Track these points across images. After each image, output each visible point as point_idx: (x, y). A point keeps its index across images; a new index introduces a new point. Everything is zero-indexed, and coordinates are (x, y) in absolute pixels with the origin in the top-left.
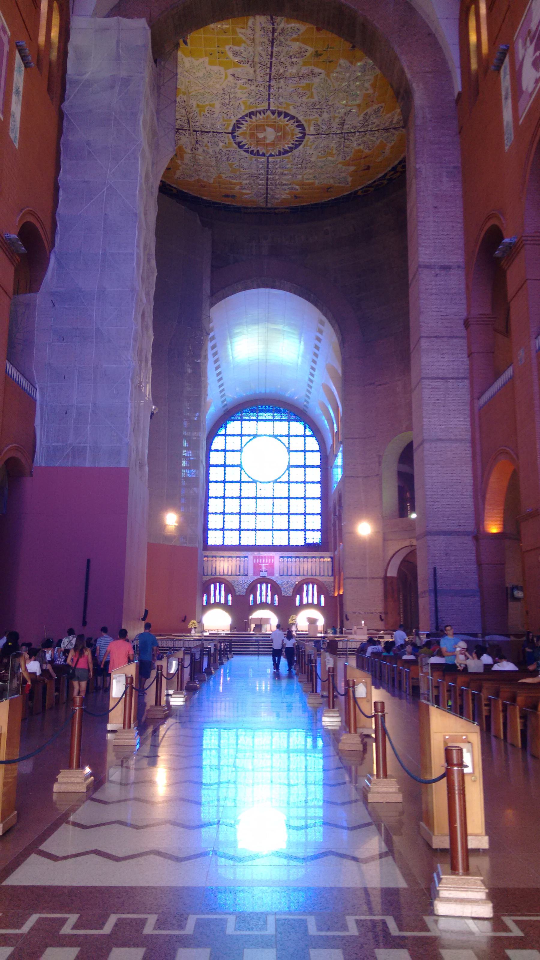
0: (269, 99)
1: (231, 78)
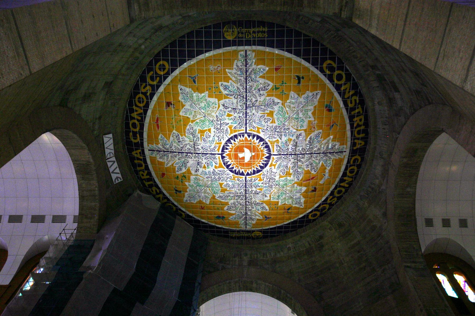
0: (246, 125)
1: (221, 107)
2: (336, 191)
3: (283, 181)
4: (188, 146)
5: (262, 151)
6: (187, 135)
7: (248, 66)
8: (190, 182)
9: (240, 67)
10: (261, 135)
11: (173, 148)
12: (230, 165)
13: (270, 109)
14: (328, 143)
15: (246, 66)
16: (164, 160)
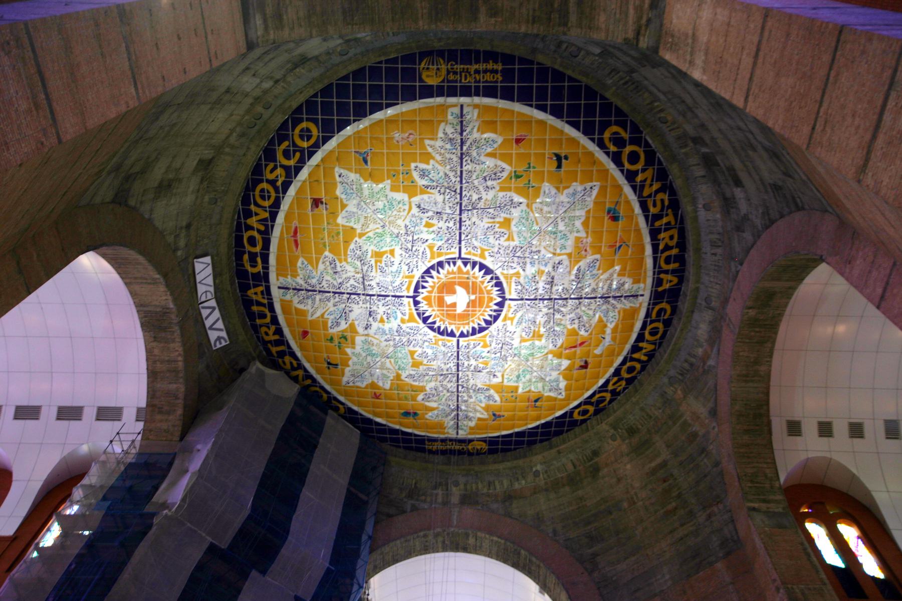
0: (460, 242)
1: (415, 210)
2: (625, 367)
3: (527, 348)
4: (352, 282)
5: (489, 292)
6: (349, 260)
7: (465, 134)
8: (354, 348)
9: (451, 136)
10: (488, 262)
11: (324, 283)
12: (429, 317)
13: (505, 215)
14: (610, 279)
15: (461, 134)
16: (307, 307)
